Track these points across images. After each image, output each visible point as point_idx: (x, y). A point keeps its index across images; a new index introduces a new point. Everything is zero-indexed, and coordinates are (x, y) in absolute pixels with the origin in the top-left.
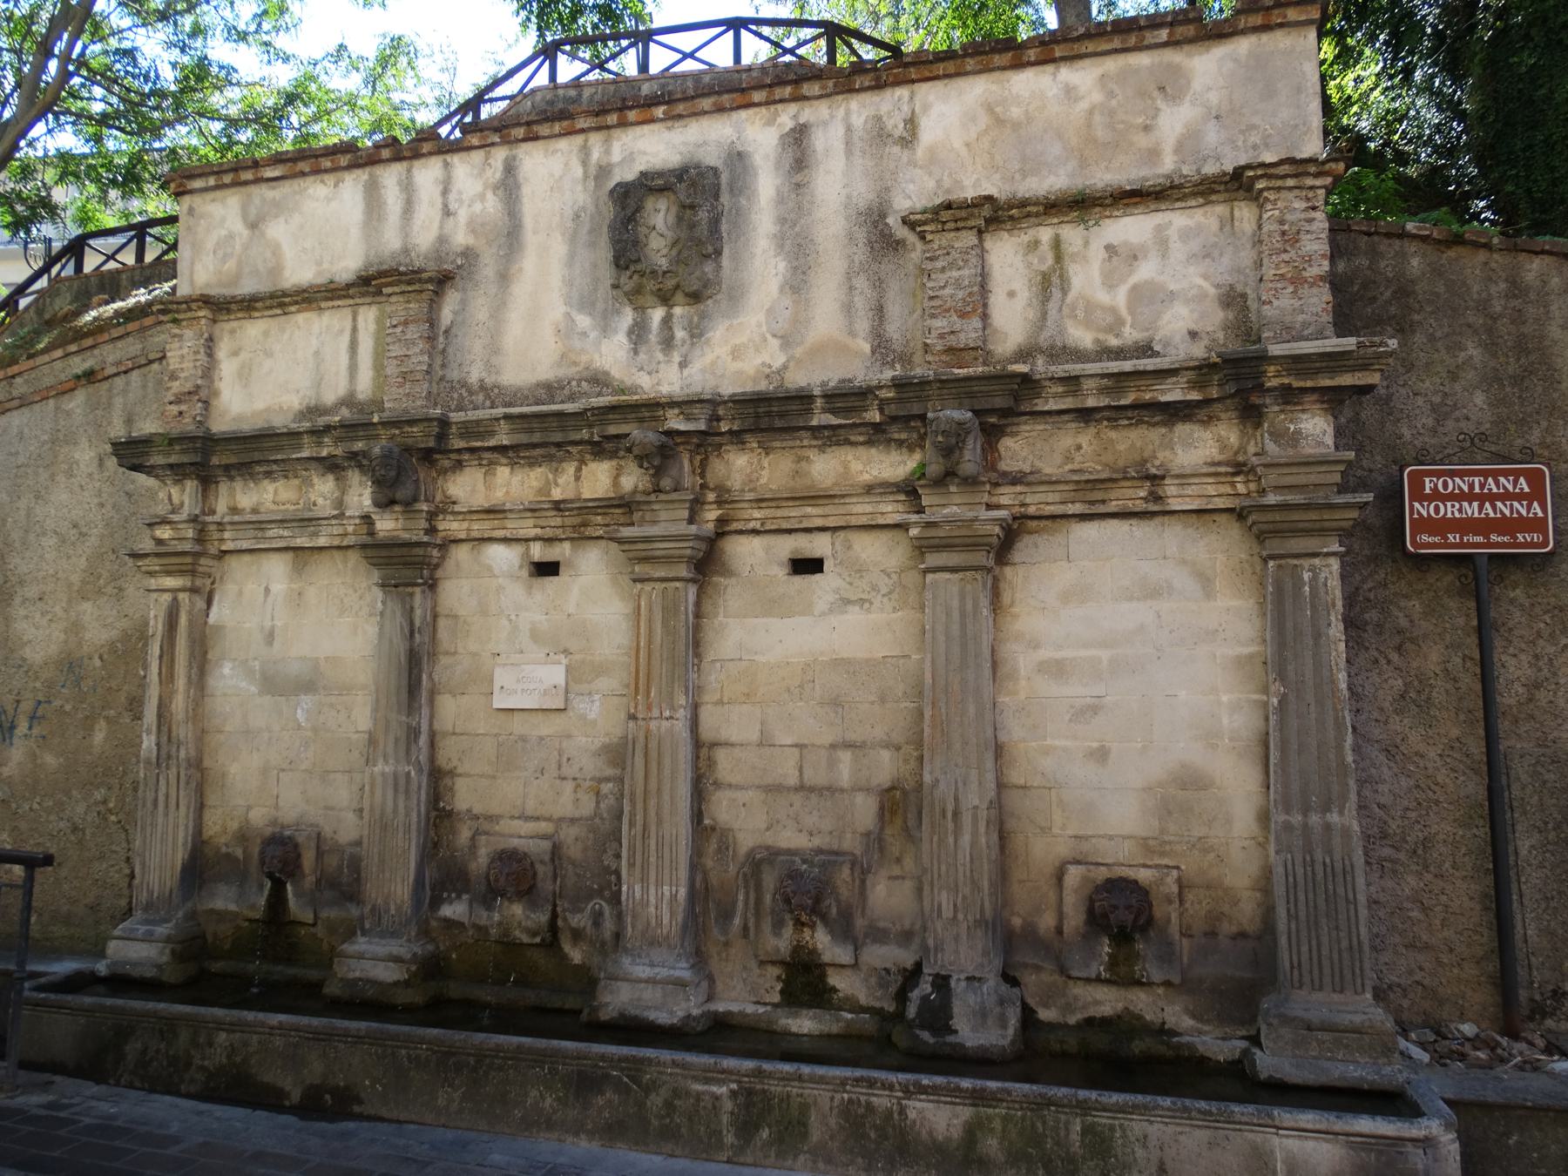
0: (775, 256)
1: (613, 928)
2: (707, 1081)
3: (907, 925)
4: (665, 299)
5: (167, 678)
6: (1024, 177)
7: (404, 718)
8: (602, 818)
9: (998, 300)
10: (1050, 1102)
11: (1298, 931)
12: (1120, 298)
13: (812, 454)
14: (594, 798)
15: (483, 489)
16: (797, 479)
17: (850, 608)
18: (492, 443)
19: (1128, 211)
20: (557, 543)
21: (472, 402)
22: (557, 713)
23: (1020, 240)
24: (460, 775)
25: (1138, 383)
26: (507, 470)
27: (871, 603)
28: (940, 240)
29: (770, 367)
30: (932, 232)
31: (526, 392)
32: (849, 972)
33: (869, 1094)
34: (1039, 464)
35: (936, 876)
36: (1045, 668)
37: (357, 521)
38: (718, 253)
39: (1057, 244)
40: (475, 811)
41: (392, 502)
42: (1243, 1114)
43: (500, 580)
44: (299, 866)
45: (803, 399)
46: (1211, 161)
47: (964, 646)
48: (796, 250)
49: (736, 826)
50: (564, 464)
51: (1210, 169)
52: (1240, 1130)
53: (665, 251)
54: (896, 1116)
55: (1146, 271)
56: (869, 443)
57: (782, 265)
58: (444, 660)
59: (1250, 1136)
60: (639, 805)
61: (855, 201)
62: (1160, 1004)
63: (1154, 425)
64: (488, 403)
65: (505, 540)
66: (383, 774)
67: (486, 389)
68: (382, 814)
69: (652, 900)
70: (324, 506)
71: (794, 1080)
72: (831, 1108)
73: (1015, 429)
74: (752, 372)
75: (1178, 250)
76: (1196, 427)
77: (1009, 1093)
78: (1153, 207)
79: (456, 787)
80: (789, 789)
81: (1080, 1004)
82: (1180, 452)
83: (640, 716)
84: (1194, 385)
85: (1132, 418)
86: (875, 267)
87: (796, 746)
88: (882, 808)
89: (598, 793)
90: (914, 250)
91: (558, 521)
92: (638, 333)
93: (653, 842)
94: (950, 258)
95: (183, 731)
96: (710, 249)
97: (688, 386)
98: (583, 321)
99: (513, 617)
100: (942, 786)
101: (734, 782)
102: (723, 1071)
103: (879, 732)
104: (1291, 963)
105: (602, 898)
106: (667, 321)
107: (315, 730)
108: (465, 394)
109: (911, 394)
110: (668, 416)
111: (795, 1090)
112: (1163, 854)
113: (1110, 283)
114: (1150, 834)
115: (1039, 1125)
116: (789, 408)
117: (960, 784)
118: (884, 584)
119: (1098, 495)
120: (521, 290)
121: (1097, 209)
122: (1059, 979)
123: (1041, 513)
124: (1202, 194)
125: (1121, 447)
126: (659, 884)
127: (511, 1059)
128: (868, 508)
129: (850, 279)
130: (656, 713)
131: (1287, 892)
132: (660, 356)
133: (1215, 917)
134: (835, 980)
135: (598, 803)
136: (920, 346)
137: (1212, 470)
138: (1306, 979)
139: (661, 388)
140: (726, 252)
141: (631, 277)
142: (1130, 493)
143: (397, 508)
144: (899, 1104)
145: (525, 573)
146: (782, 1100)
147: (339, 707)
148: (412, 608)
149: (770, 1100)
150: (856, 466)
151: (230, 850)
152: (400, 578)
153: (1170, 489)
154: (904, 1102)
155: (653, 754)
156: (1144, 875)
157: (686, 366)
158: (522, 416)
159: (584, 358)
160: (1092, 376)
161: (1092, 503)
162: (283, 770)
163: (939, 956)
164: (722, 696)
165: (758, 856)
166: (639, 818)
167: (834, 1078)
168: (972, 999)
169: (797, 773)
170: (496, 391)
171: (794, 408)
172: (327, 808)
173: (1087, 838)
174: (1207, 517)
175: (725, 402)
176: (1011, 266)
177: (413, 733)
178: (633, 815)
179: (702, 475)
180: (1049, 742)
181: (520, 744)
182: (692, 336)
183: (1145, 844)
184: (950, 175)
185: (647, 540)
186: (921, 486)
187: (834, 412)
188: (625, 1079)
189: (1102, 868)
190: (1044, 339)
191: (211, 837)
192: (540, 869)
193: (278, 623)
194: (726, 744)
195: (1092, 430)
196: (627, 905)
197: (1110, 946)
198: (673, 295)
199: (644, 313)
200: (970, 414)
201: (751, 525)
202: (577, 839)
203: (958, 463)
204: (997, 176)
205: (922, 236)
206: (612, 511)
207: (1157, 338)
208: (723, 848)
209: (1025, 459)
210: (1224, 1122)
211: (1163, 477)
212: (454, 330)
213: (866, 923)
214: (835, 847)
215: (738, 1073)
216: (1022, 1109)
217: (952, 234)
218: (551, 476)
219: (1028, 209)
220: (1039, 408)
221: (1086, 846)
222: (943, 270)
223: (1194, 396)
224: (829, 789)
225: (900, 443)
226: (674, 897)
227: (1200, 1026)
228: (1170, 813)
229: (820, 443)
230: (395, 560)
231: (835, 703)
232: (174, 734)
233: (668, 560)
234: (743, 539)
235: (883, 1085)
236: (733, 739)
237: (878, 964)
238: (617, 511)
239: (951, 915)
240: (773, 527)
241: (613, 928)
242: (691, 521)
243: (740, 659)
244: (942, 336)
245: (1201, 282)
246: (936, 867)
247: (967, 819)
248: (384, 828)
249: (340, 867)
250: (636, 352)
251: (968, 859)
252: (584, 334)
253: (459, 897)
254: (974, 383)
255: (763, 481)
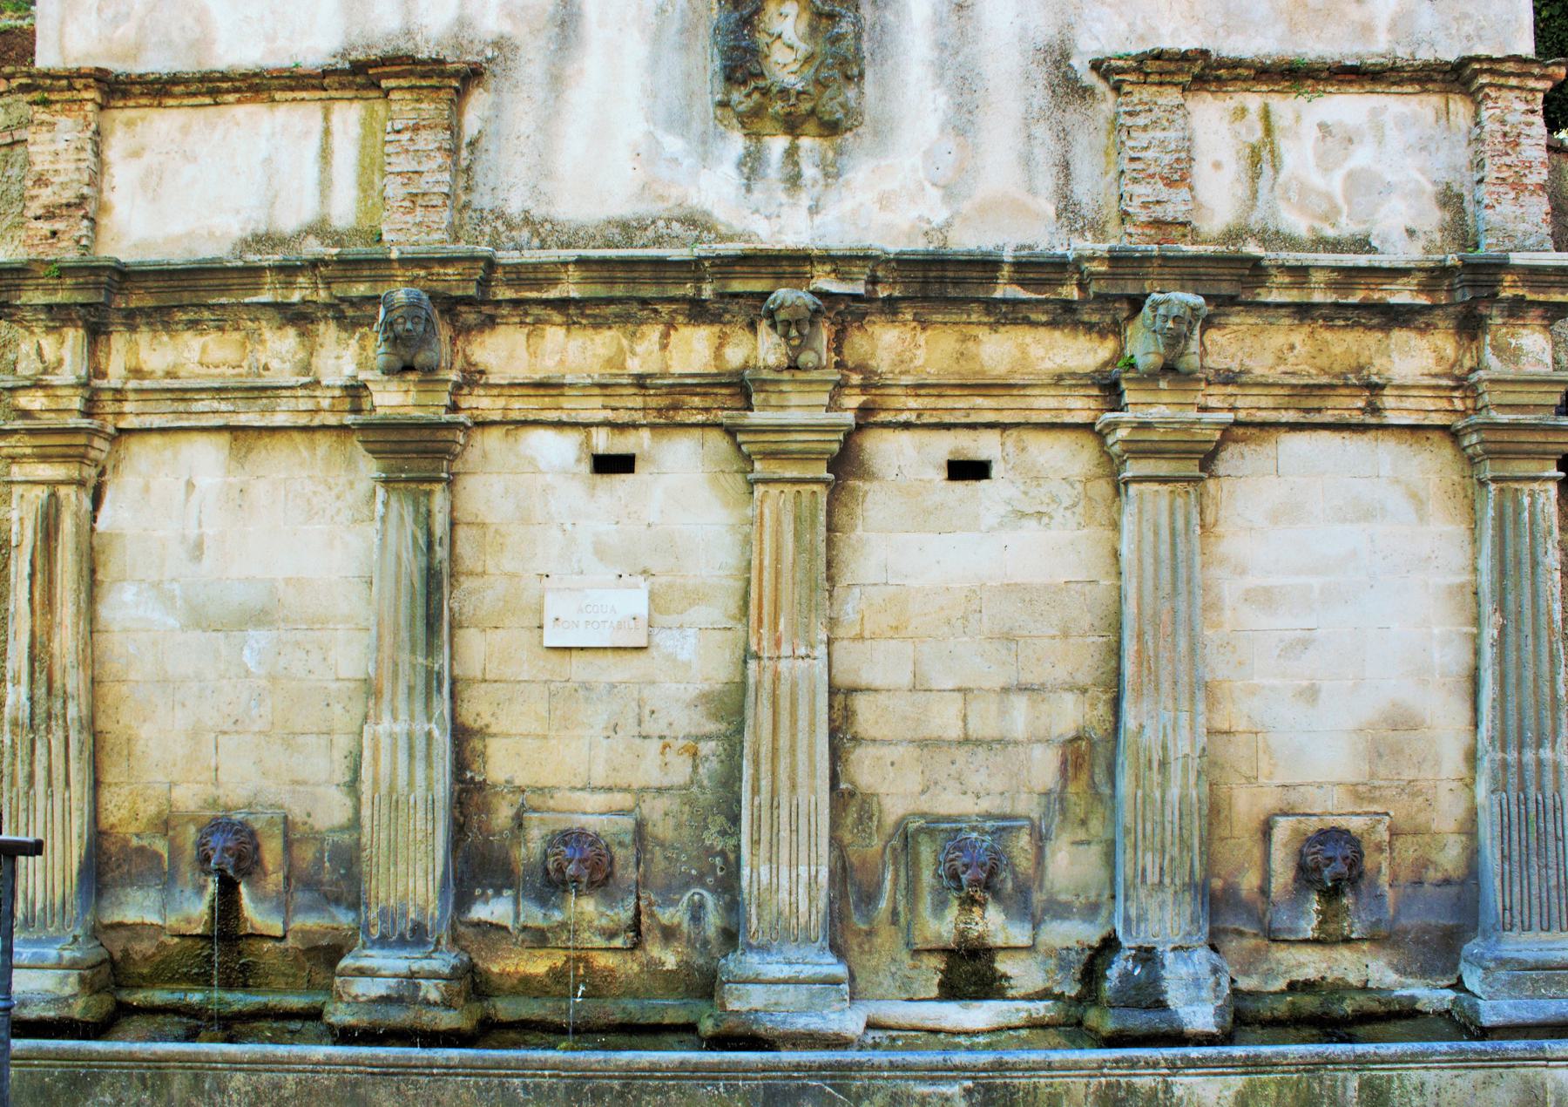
0: (934, 88)
1: (718, 922)
2: (934, 1081)
3: (1093, 898)
4: (792, 126)
5: (45, 603)
6: (1229, 34)
7: (421, 660)
8: (701, 787)
9: (1202, 171)
10: (1329, 1061)
11: (1510, 872)
12: (1335, 184)
13: (983, 333)
14: (690, 761)
15: (525, 355)
16: (962, 362)
17: (1025, 522)
18: (553, 294)
19: (1343, 88)
20: (633, 432)
21: (512, 239)
22: (635, 653)
23: (1225, 105)
24: (494, 735)
25: (1369, 281)
26: (561, 331)
27: (1051, 518)
28: (1141, 93)
29: (929, 222)
30: (1132, 83)
31: (591, 231)
32: (1023, 955)
33: (1130, 1075)
34: (1249, 363)
35: (1140, 837)
36: (1249, 596)
37: (337, 393)
38: (861, 75)
39: (1266, 115)
40: (517, 783)
41: (408, 368)
42: (1516, 1050)
43: (549, 477)
44: (258, 862)
45: (987, 266)
46: (1425, 46)
47: (1174, 570)
48: (959, 83)
49: (882, 790)
50: (644, 328)
51: (1425, 55)
52: (1513, 1066)
53: (795, 67)
54: (1161, 1095)
55: (1362, 157)
56: (1053, 324)
57: (943, 100)
58: (466, 583)
59: (1523, 1070)
60: (765, 767)
61: (1031, 34)
62: (1365, 961)
63: (1371, 328)
64: (536, 242)
65: (559, 425)
66: (392, 736)
67: (533, 223)
68: (392, 788)
69: (784, 883)
70: (282, 371)
71: (1041, 1069)
72: (1086, 1097)
73: (1223, 320)
74: (905, 226)
75: (1394, 139)
76: (1412, 334)
77: (1285, 1056)
78: (1368, 88)
79: (489, 751)
80: (950, 743)
81: (1283, 968)
82: (1397, 360)
83: (765, 655)
84: (1424, 288)
85: (1348, 319)
86: (1058, 115)
87: (959, 690)
88: (1064, 763)
89: (695, 754)
90: (1104, 100)
91: (638, 402)
92: (751, 166)
93: (784, 813)
94: (1153, 116)
95: (73, 681)
96: (856, 71)
97: (821, 237)
98: (673, 144)
99: (568, 526)
100: (1148, 732)
101: (879, 736)
102: (956, 1068)
103: (1061, 673)
104: (1504, 906)
105: (704, 885)
106: (791, 153)
107: (273, 678)
108: (501, 228)
109: (1127, 270)
110: (815, 273)
111: (1042, 1080)
112: (1372, 800)
113: (1325, 166)
114: (1361, 780)
115: (1316, 1086)
116: (967, 274)
117: (1169, 730)
118: (1067, 495)
119: (1315, 403)
120: (583, 96)
121: (1309, 82)
122: (1262, 942)
123: (1253, 418)
124: (1420, 81)
125: (1337, 350)
126: (793, 864)
127: (672, 1078)
128: (1053, 403)
129: (1027, 126)
130: (786, 650)
131: (1502, 832)
132: (782, 197)
133: (1424, 864)
134: (1003, 965)
135: (695, 767)
136: (1114, 214)
137: (1434, 382)
138: (1517, 920)
139: (784, 237)
140: (869, 75)
141: (749, 95)
142: (1347, 402)
143: (411, 377)
144: (1165, 1082)
145: (586, 467)
146: (1028, 1093)
147: (308, 647)
148: (429, 513)
149: (1012, 1094)
150: (1036, 351)
151: (145, 843)
152: (411, 471)
153: (1388, 401)
154: (1169, 1079)
155: (784, 704)
156: (1356, 824)
157: (817, 213)
158: (603, 262)
159: (675, 192)
160: (1322, 268)
161: (1308, 411)
162: (225, 733)
163: (1142, 926)
164: (862, 631)
165: (912, 826)
166: (765, 784)
167: (1090, 1061)
168: (1184, 971)
169: (961, 724)
170: (548, 226)
171: (974, 274)
172: (295, 782)
173: (1294, 787)
174: (1420, 434)
175: (888, 261)
176: (1216, 133)
177: (432, 680)
178: (756, 779)
179: (838, 350)
180: (1256, 680)
181: (581, 693)
182: (827, 175)
183: (1357, 792)
184: (1144, 18)
185: (783, 429)
186: (1128, 380)
187: (1022, 283)
188: (828, 1089)
189: (1314, 818)
190: (1255, 220)
191: (112, 826)
192: (619, 853)
193: (209, 531)
194: (868, 689)
195: (1306, 329)
196: (750, 893)
197: (1319, 902)
198: (802, 123)
199: (759, 140)
200: (1202, 300)
201: (903, 417)
202: (666, 814)
203: (1182, 355)
204: (1198, 28)
205: (1117, 88)
206: (716, 390)
207: (1375, 232)
208: (865, 816)
209: (1233, 357)
210: (1498, 1060)
211: (1383, 387)
212: (483, 143)
213: (1045, 897)
214: (1008, 811)
215: (975, 1068)
216: (1297, 1071)
217: (1155, 88)
218: (625, 342)
219: (1239, 71)
220: (1262, 299)
221: (1293, 796)
222: (1145, 128)
223: (1423, 300)
224: (999, 741)
225: (1090, 327)
226: (813, 881)
227: (1403, 979)
228: (1380, 756)
229: (992, 320)
230: (408, 447)
231: (1009, 638)
232: (57, 684)
233: (804, 456)
234: (888, 434)
235: (1147, 1063)
236: (877, 684)
237: (1058, 943)
238: (724, 391)
239: (1156, 880)
240: (933, 420)
241: (718, 922)
242: (829, 409)
243: (886, 584)
244: (1145, 205)
245: (1418, 176)
246: (1140, 828)
247: (1175, 769)
248: (395, 806)
249: (319, 861)
250: (749, 189)
251: (1177, 813)
252: (675, 160)
253: (498, 893)
254: (1200, 264)
255: (918, 362)
